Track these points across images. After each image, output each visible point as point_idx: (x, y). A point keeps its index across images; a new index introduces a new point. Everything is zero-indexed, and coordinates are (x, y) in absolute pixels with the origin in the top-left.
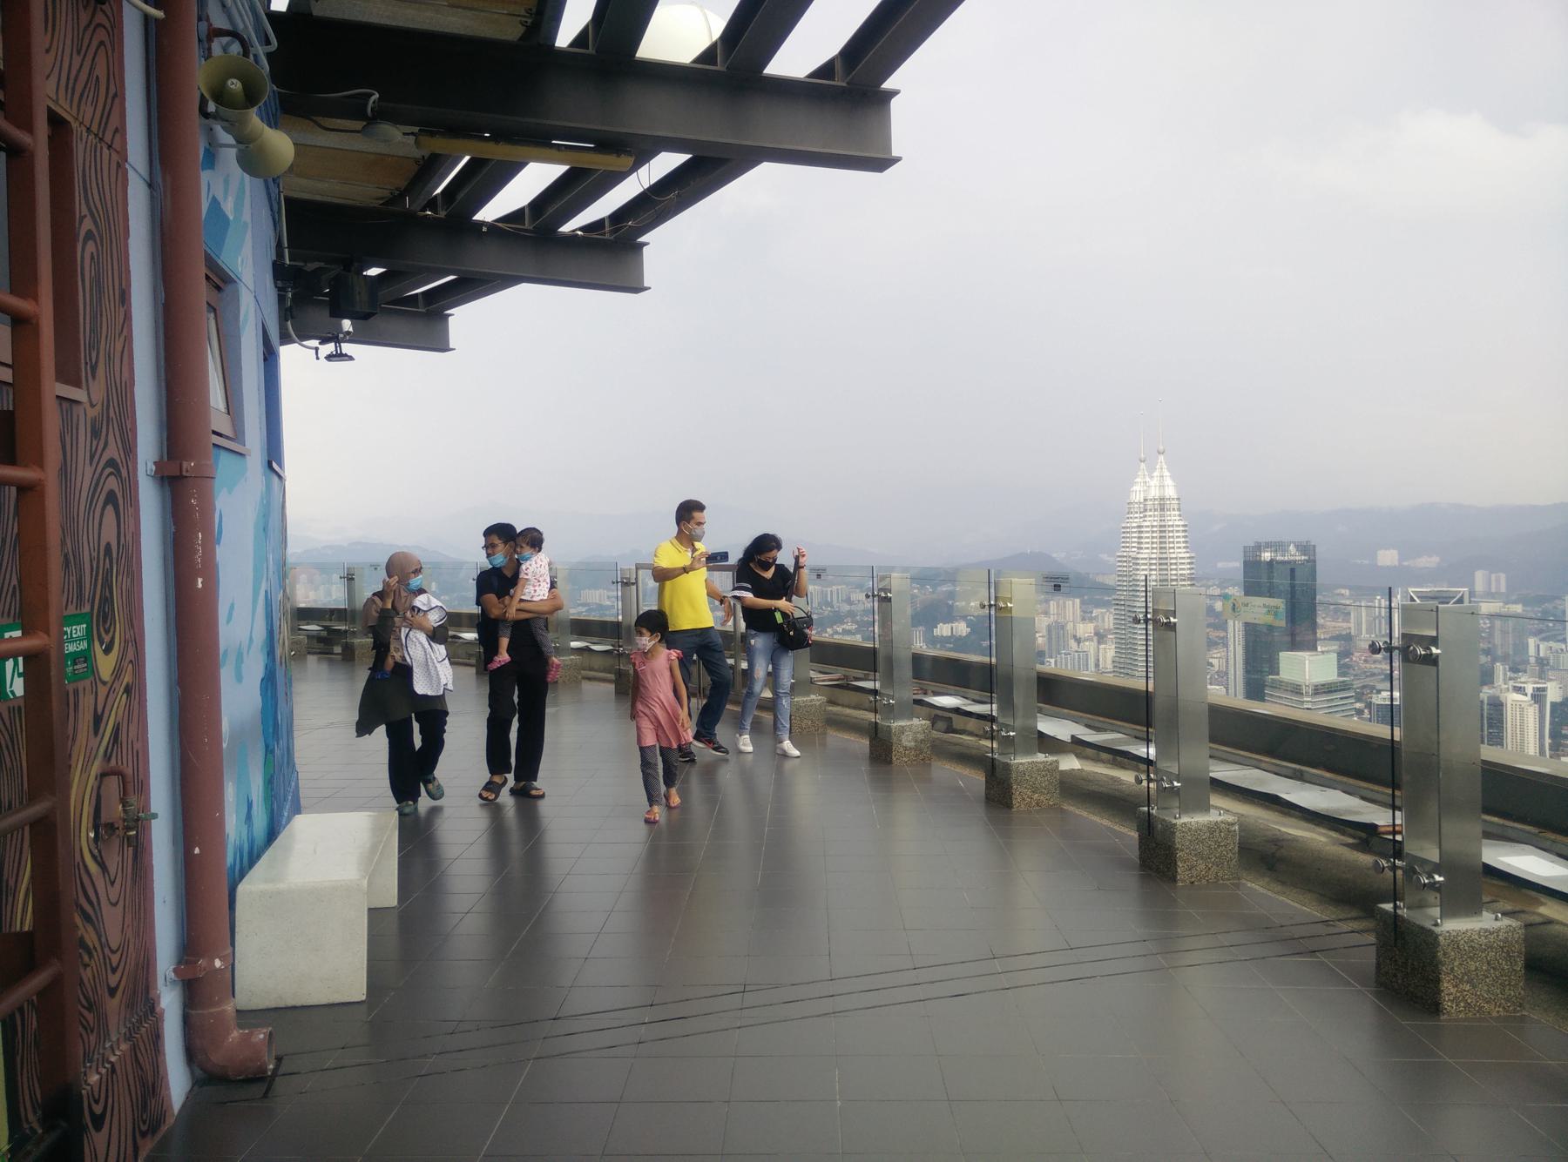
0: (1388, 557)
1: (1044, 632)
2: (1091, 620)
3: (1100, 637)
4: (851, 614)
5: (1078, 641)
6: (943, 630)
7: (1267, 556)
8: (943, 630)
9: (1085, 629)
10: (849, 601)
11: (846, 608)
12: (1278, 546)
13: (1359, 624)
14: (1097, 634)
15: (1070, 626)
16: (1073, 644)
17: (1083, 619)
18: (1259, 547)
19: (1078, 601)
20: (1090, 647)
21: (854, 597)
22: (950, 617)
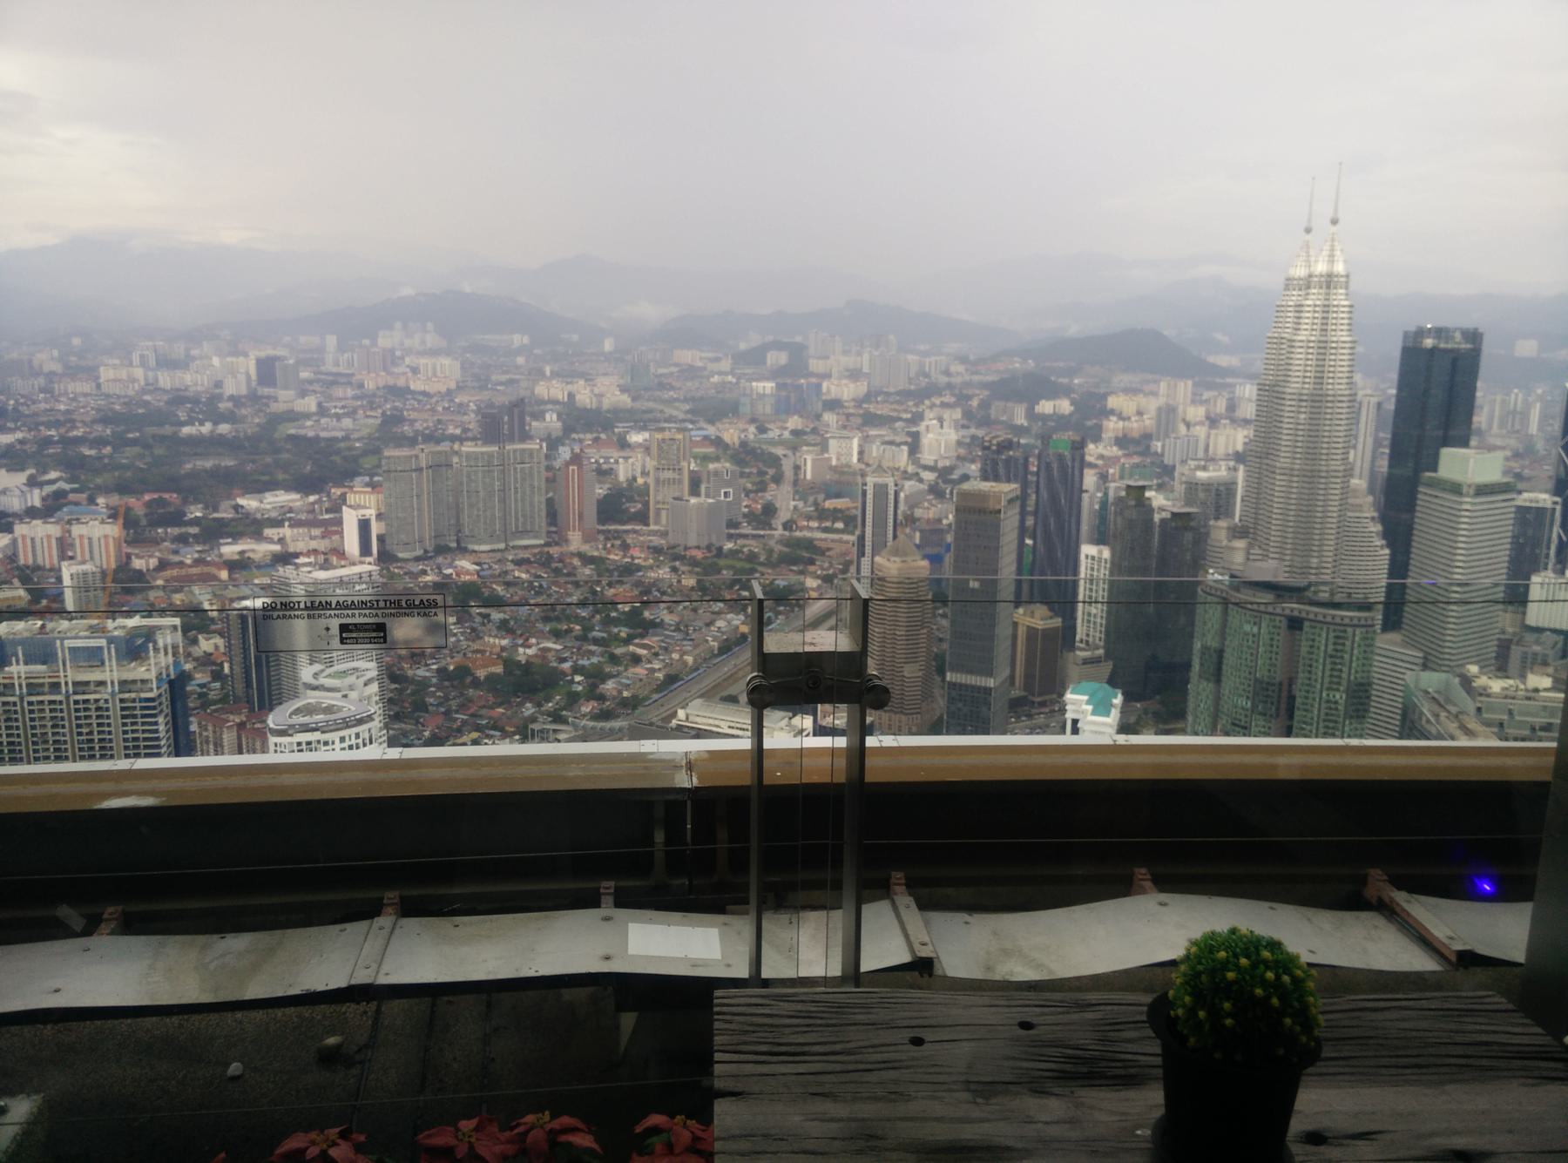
0: (1527, 348)
1: (1153, 413)
2: (1202, 402)
3: (1213, 421)
4: (950, 386)
5: (1188, 425)
6: (1046, 407)
7: (1429, 342)
8: (1046, 407)
9: (1196, 413)
10: (947, 373)
11: (944, 380)
12: (1439, 332)
13: (1491, 419)
14: (1208, 418)
15: (1181, 408)
16: (1182, 429)
17: (1193, 402)
18: (1421, 333)
19: (1190, 383)
20: (1201, 431)
21: (953, 369)
22: (1055, 392)
